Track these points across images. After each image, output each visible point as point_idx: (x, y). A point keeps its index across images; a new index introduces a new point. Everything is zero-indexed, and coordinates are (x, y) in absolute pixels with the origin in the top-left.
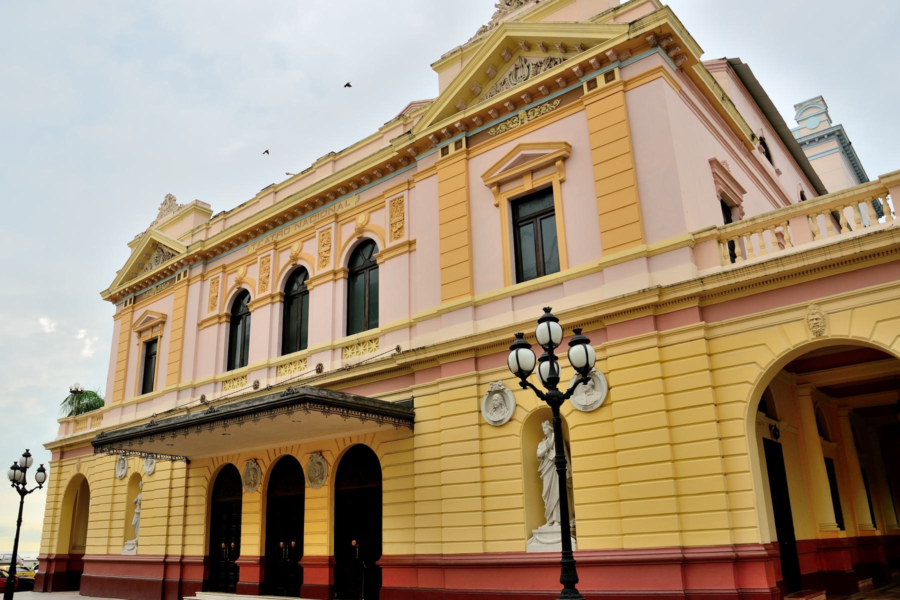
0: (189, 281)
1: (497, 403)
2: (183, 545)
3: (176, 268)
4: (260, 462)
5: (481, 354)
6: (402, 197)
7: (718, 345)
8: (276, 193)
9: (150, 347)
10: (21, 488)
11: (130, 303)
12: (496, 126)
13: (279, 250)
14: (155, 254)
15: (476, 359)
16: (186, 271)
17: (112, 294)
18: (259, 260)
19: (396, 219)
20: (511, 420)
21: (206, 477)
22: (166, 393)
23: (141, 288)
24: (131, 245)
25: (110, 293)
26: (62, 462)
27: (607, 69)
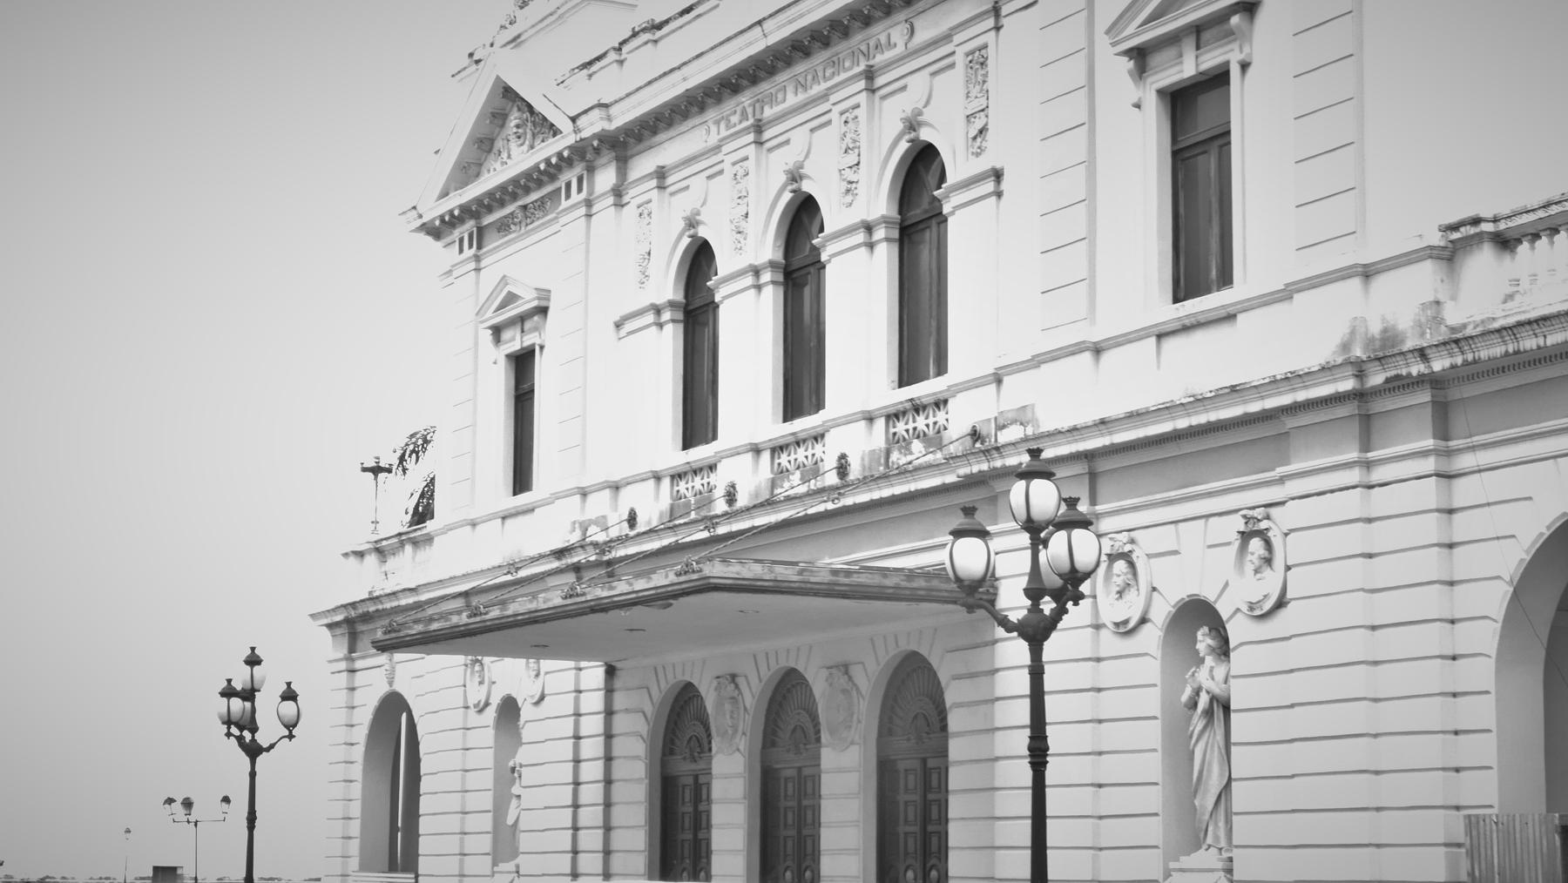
0: (589, 203)
1: (1120, 581)
3: (558, 168)
4: (741, 681)
5: (1103, 465)
6: (985, 47)
7: (1464, 491)
9: (522, 363)
10: (247, 741)
11: (471, 246)
13: (768, 145)
14: (513, 120)
16: (582, 175)
17: (425, 219)
18: (726, 166)
20: (1143, 620)
21: (644, 713)
22: (557, 497)
23: (490, 209)
25: (420, 216)
26: (353, 660)
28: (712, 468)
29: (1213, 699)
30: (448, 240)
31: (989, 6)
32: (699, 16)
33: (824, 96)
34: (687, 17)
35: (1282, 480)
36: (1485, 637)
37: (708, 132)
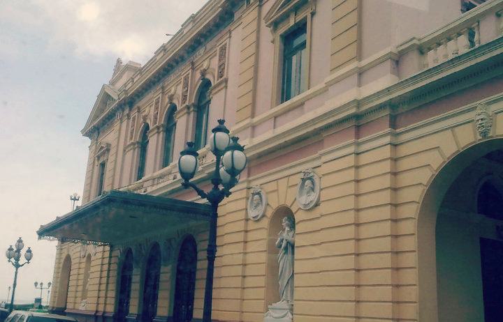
0: (121, 119)
9: (103, 165)
19: (221, 63)
20: (264, 216)
29: (288, 242)
35: (319, 158)
36: (411, 211)
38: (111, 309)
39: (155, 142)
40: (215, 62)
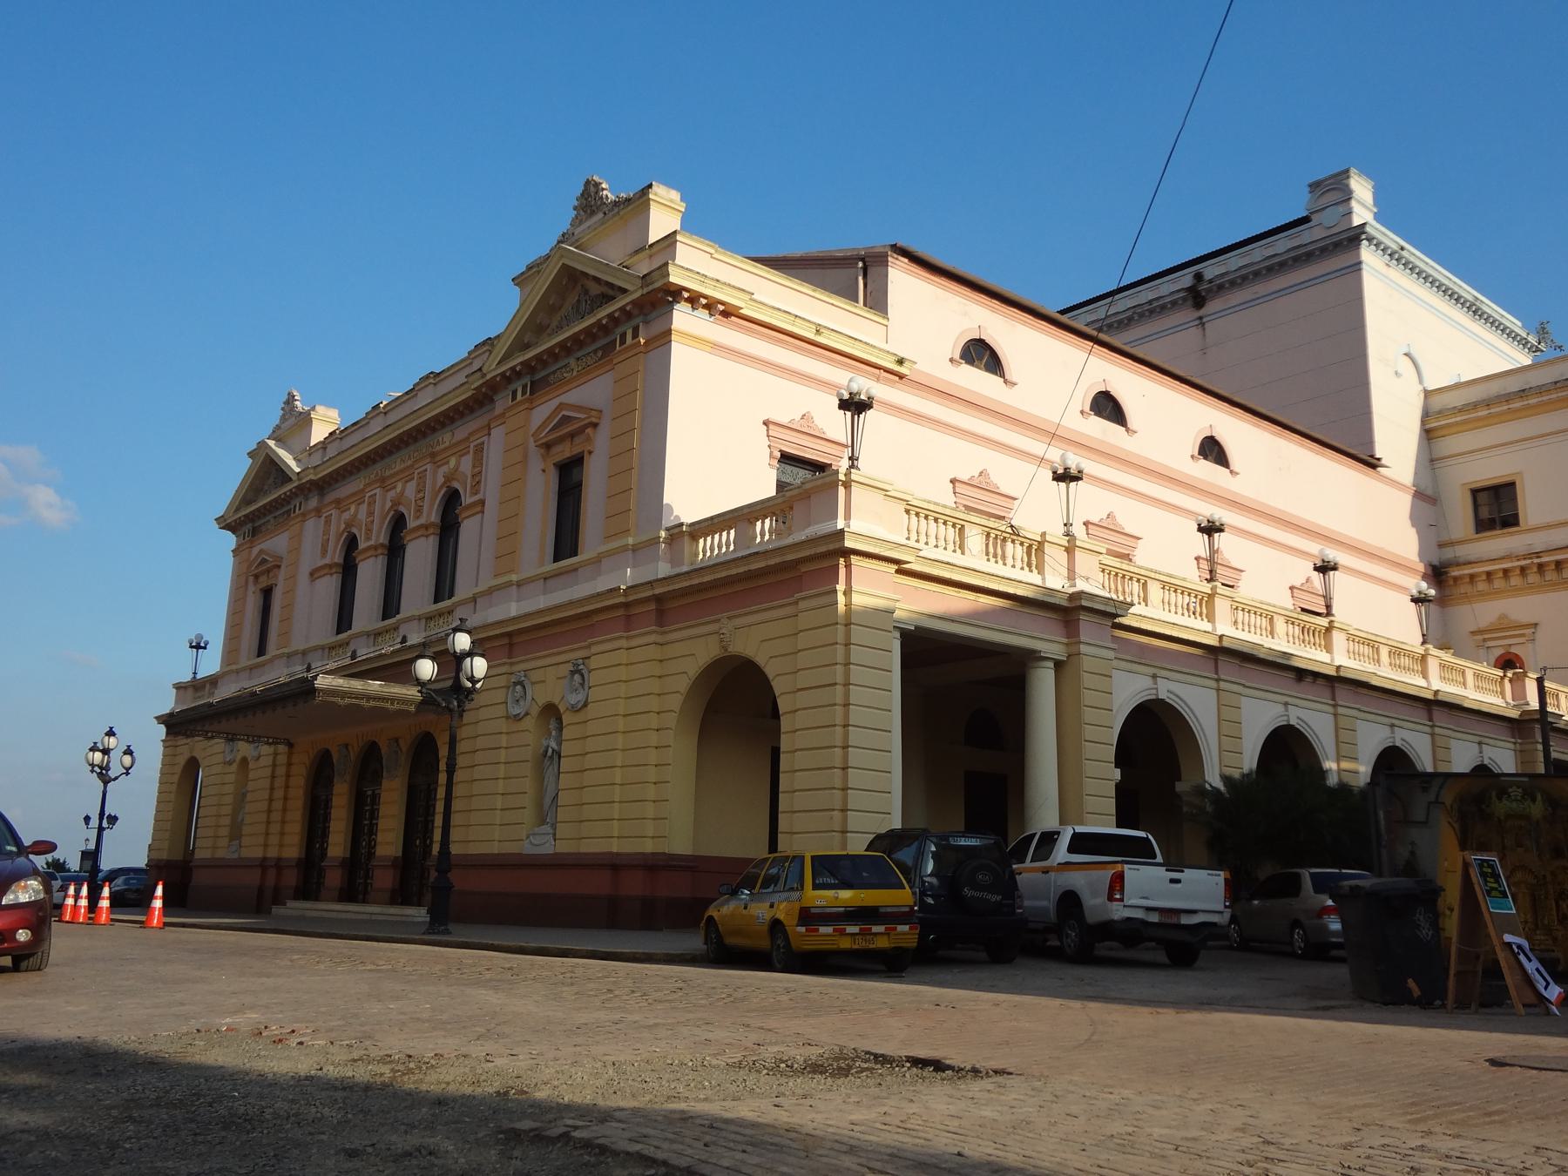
0: (304, 515)
1: (518, 695)
2: (281, 846)
4: (350, 748)
5: (516, 640)
8: (385, 413)
9: (267, 593)
12: (554, 372)
15: (511, 645)
18: (366, 499)
20: (527, 714)
23: (259, 518)
24: (251, 455)
25: (225, 520)
27: (634, 322)
28: (348, 644)
30: (238, 533)
31: (486, 423)
32: (361, 427)
33: (412, 466)
34: (356, 427)
35: (589, 647)
37: (361, 482)
38: (292, 850)
39: (370, 574)
40: (466, 464)
